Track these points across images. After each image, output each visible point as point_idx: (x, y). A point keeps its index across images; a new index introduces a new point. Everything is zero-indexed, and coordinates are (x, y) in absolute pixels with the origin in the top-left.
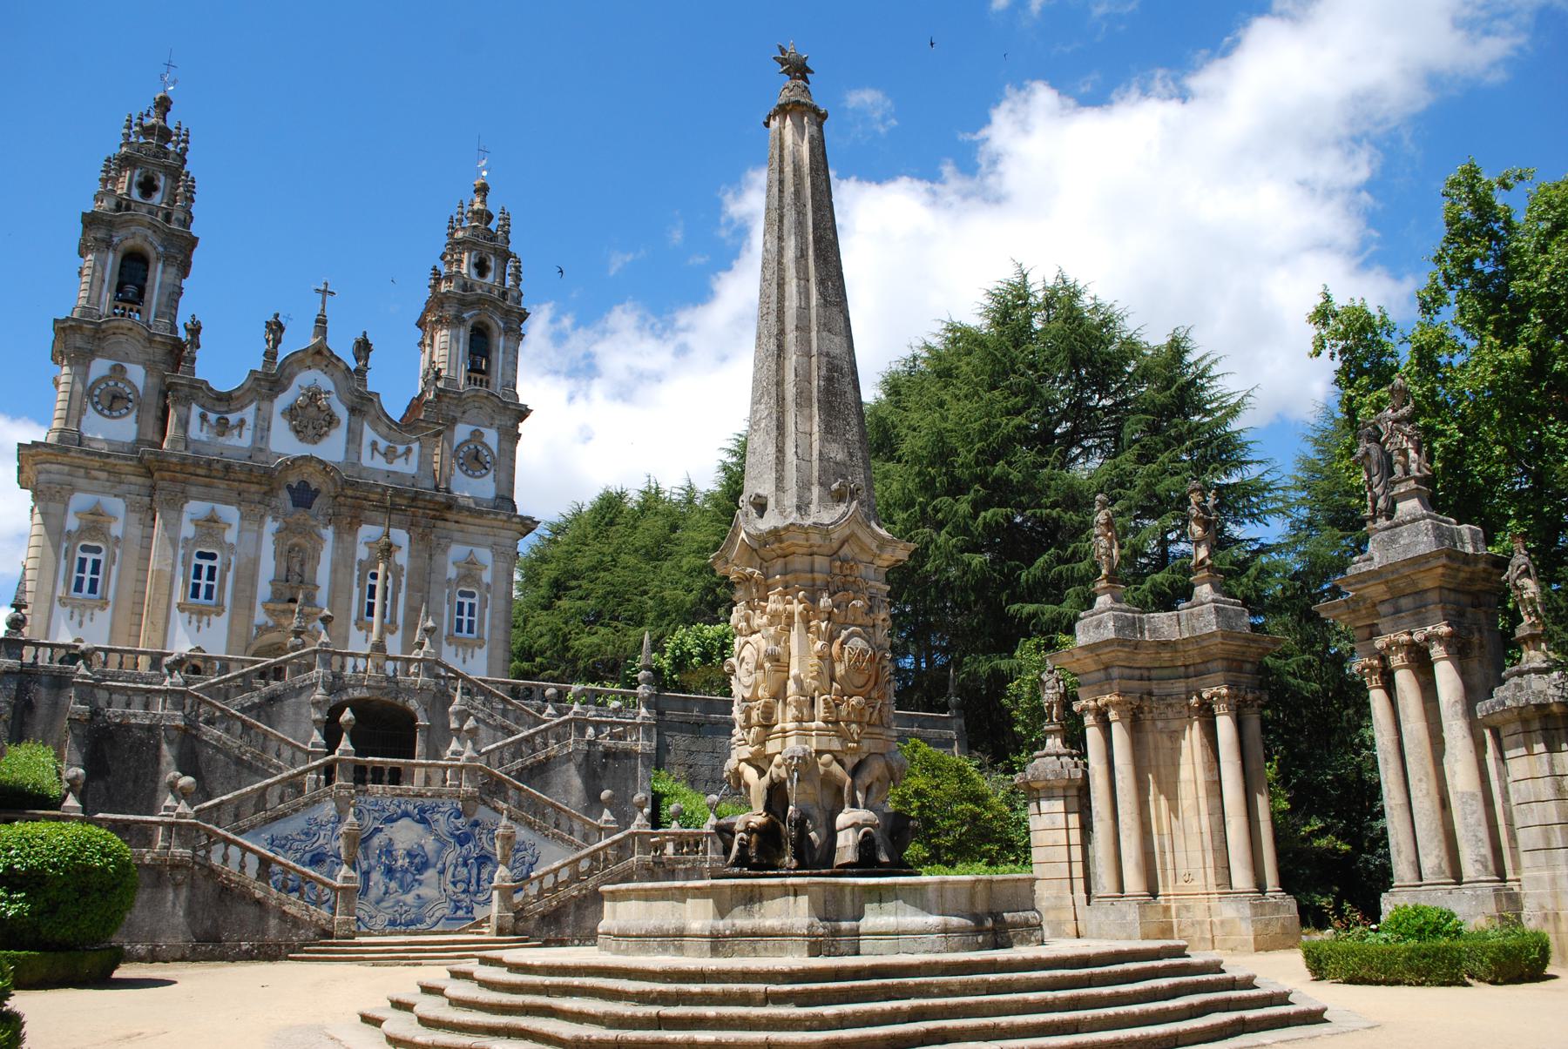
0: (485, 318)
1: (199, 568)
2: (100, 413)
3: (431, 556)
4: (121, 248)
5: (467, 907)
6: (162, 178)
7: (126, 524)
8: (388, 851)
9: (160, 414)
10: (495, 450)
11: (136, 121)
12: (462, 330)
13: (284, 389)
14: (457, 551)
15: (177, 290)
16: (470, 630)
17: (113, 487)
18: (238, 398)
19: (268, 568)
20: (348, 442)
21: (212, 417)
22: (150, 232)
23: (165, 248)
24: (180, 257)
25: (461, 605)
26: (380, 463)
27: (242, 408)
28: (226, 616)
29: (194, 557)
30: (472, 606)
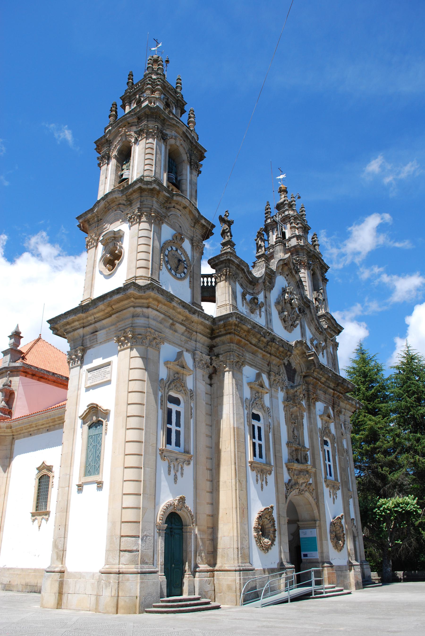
7: (195, 379)
17: (186, 342)
21: (248, 297)
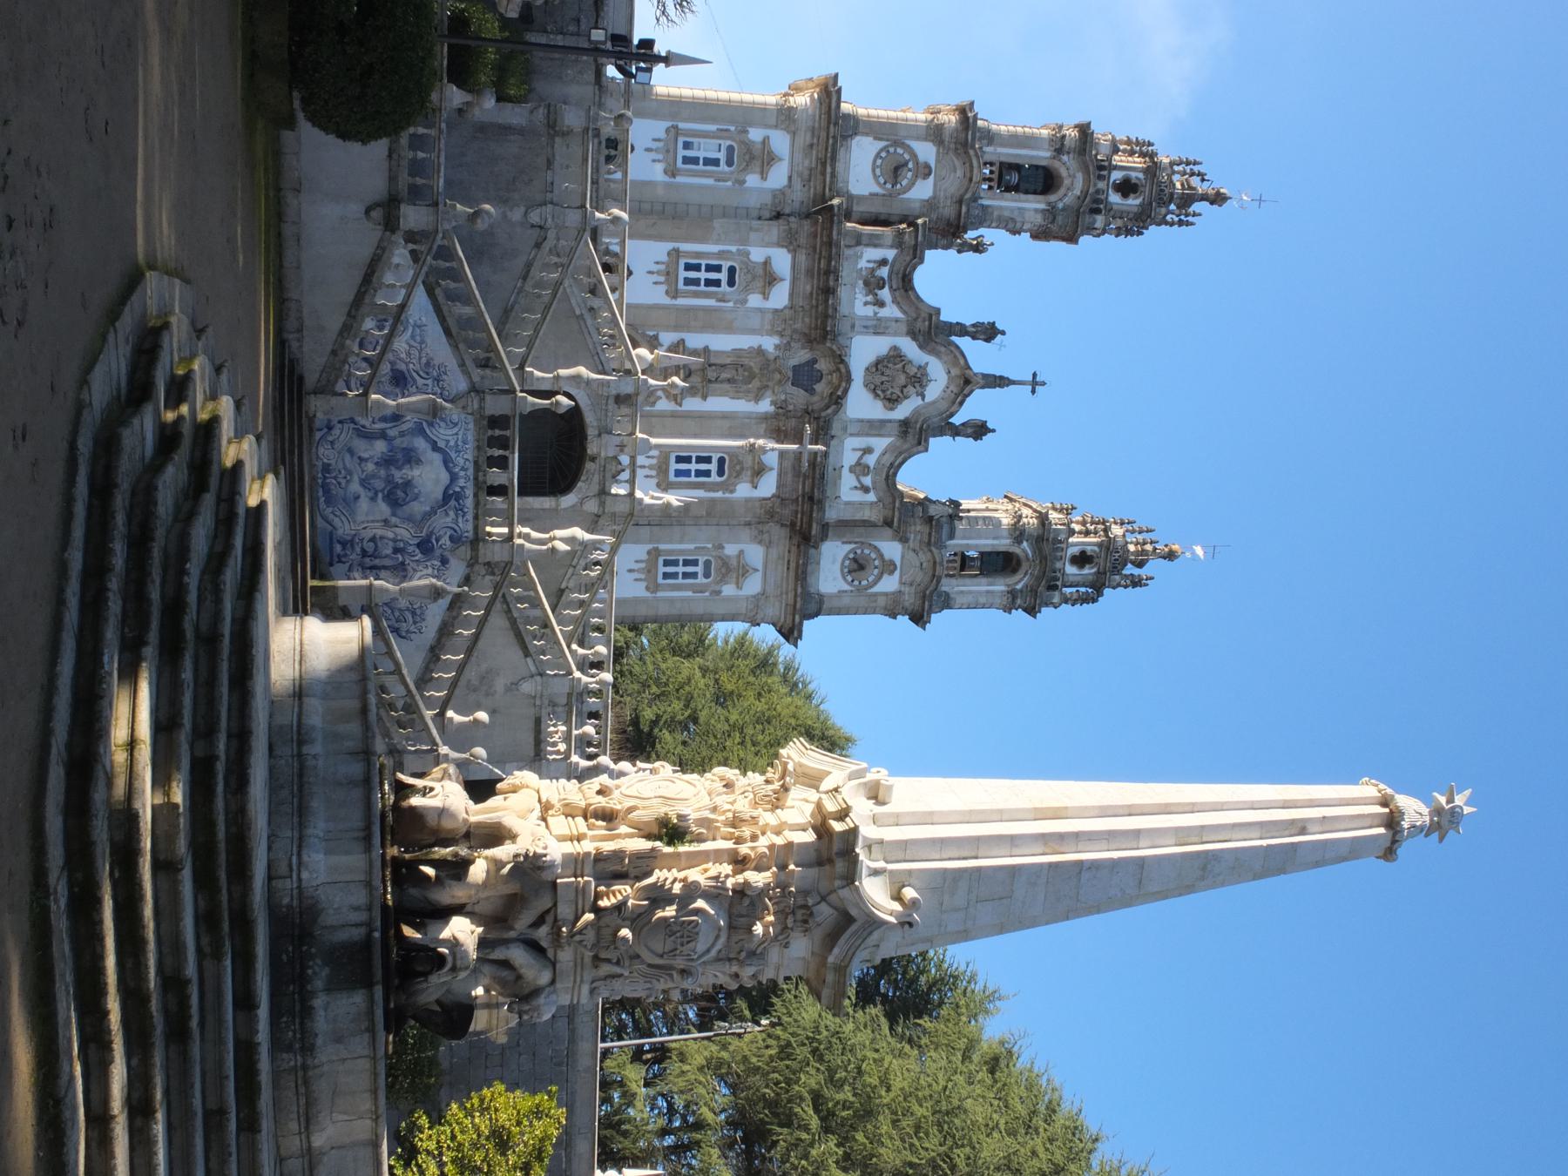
0: (1025, 566)
1: (718, 269)
2: (878, 155)
3: (748, 524)
4: (1056, 164)
5: (346, 555)
6: (1138, 202)
7: (761, 191)
8: (411, 458)
9: (882, 217)
10: (875, 589)
11: (1196, 168)
12: (1008, 541)
13: (921, 347)
14: (755, 554)
15: (1018, 226)
16: (666, 576)
17: (800, 175)
18: (908, 297)
19: (722, 343)
20: (869, 421)
21: (884, 272)
22: (1077, 192)
23: (1063, 209)
24: (1054, 228)
25: (695, 563)
26: (849, 458)
27: (894, 301)
28: (667, 301)
29: (730, 263)
30: (694, 575)
